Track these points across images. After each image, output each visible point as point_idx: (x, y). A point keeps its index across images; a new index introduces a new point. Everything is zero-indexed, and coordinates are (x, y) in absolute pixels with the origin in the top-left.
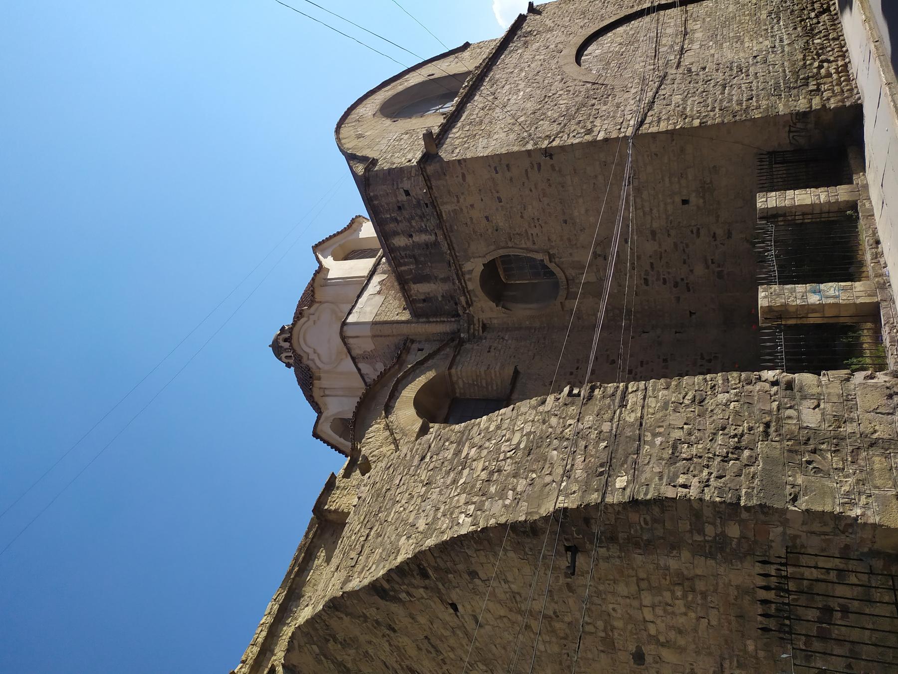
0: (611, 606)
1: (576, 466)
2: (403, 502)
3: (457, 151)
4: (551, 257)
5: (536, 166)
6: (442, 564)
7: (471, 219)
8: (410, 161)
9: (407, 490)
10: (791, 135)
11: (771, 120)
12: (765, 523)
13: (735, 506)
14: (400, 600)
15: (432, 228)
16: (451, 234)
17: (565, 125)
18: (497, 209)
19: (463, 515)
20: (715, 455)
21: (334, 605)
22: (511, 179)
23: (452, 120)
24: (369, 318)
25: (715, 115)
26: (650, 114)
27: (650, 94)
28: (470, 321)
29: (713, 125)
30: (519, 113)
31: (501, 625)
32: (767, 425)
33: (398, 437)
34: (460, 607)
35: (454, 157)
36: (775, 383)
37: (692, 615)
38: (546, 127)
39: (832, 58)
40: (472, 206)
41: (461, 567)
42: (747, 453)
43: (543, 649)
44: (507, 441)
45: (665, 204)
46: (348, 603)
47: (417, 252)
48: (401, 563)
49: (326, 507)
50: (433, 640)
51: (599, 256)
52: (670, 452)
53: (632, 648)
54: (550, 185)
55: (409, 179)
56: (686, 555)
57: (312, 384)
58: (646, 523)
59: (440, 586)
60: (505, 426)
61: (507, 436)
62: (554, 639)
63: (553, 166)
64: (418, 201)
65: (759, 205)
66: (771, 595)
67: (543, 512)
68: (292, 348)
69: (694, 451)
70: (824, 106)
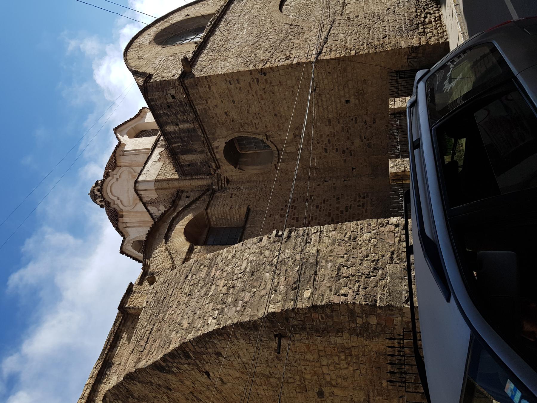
0: (303, 367)
1: (280, 284)
2: (174, 307)
3: (205, 70)
4: (267, 137)
5: (255, 80)
6: (198, 350)
7: (216, 114)
8: (174, 76)
9: (177, 298)
10: (409, 60)
11: (397, 52)
12: (391, 315)
13: (374, 306)
15: (191, 119)
16: (203, 124)
17: (273, 53)
18: (232, 108)
19: (211, 318)
20: (362, 274)
21: (130, 377)
22: (240, 89)
23: (201, 48)
24: (153, 177)
25: (364, 48)
26: (325, 46)
27: (325, 33)
28: (219, 178)
29: (363, 55)
30: (244, 44)
31: (237, 382)
32: (393, 253)
33: (174, 256)
34: (211, 374)
35: (202, 74)
36: (397, 226)
37: (351, 369)
38: (261, 54)
39: (432, 12)
40: (216, 106)
41: (210, 350)
42: (380, 271)
43: (263, 393)
44: (238, 266)
45: (336, 103)
46: (140, 375)
47: (182, 135)
48: (173, 350)
49: (127, 306)
51: (297, 135)
52: (336, 273)
54: (265, 92)
55: (174, 87)
56: (346, 335)
57: (117, 220)
58: (322, 318)
59: (198, 362)
60: (237, 256)
61: (239, 263)
62: (270, 388)
63: (266, 80)
65: (390, 106)
66: (396, 360)
68: (102, 196)
69: (350, 271)
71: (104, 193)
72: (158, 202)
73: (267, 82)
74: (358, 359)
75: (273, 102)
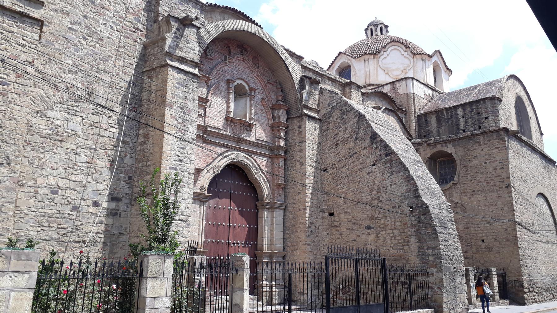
4: (455, 184)
7: (475, 149)
14: (372, 144)
34: (374, 167)
37: (392, 245)
40: (482, 150)
41: (394, 169)
43: (363, 195)
50: (355, 156)
53: (372, 226)
59: (383, 160)
62: (369, 200)
63: (502, 188)
64: (482, 123)
65: (493, 268)
67: (424, 200)
70: (525, 293)
71: (393, 43)
72: (394, 93)
73: (500, 188)
74: (400, 249)
75: (484, 190)
